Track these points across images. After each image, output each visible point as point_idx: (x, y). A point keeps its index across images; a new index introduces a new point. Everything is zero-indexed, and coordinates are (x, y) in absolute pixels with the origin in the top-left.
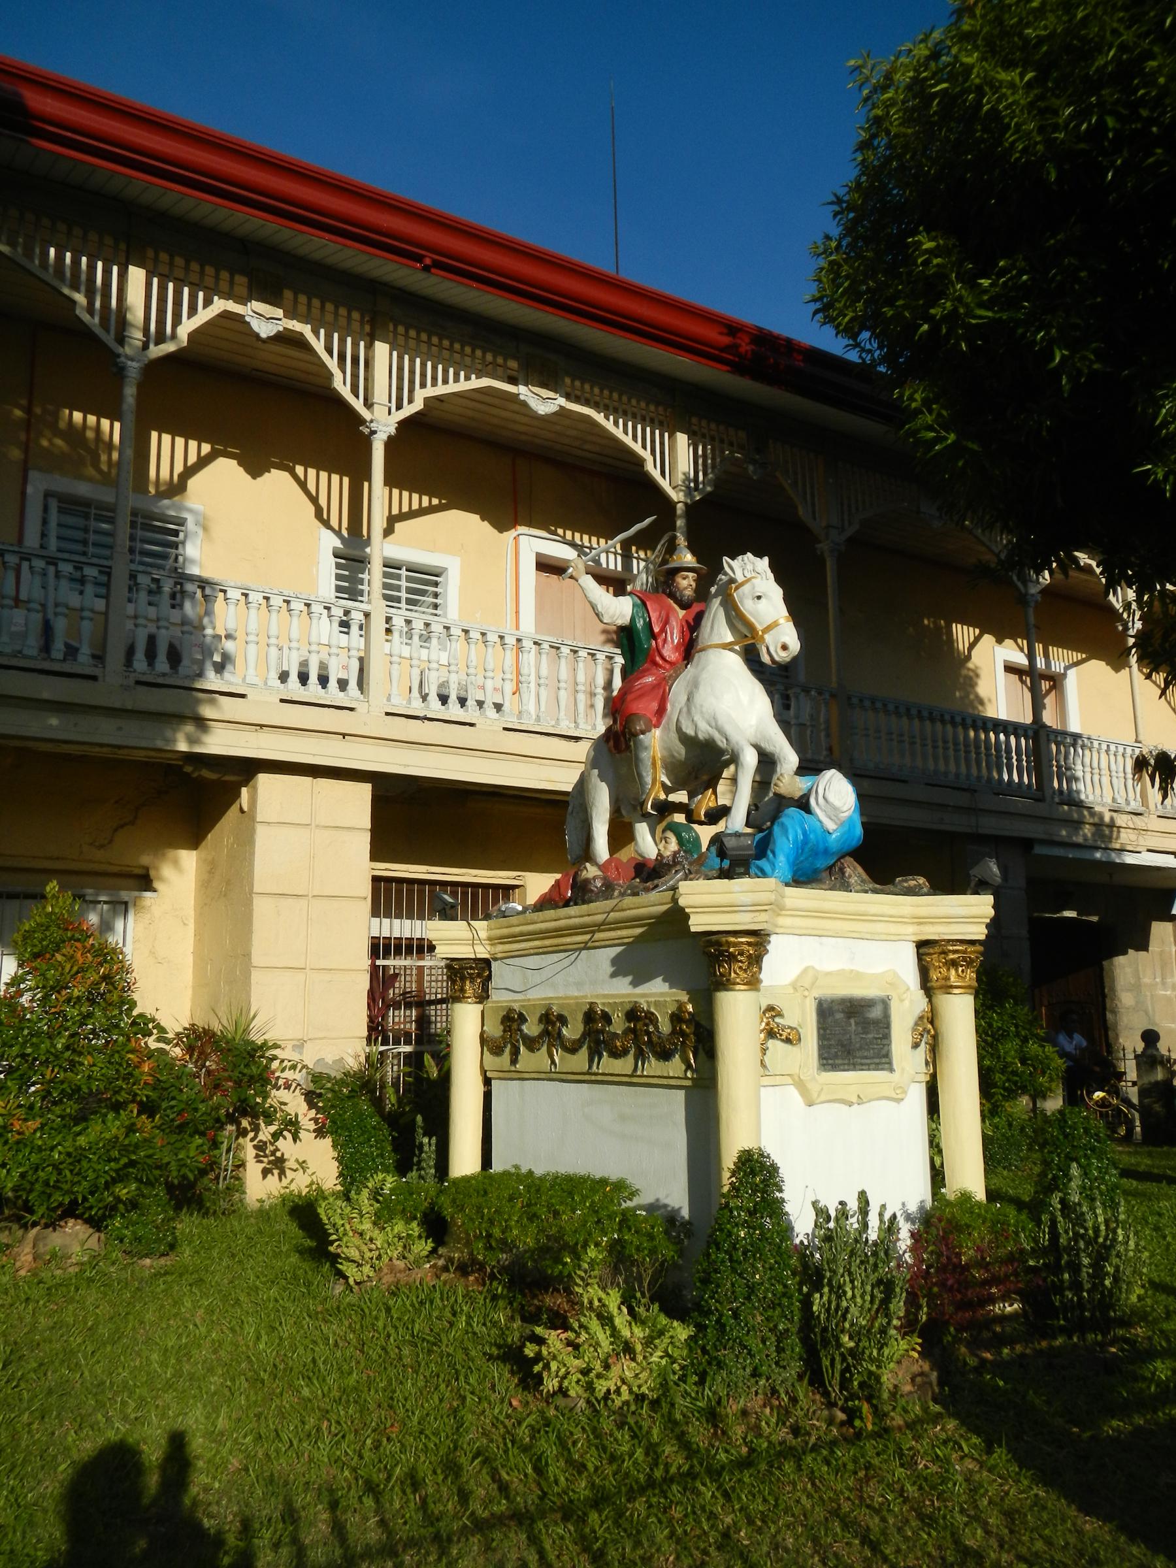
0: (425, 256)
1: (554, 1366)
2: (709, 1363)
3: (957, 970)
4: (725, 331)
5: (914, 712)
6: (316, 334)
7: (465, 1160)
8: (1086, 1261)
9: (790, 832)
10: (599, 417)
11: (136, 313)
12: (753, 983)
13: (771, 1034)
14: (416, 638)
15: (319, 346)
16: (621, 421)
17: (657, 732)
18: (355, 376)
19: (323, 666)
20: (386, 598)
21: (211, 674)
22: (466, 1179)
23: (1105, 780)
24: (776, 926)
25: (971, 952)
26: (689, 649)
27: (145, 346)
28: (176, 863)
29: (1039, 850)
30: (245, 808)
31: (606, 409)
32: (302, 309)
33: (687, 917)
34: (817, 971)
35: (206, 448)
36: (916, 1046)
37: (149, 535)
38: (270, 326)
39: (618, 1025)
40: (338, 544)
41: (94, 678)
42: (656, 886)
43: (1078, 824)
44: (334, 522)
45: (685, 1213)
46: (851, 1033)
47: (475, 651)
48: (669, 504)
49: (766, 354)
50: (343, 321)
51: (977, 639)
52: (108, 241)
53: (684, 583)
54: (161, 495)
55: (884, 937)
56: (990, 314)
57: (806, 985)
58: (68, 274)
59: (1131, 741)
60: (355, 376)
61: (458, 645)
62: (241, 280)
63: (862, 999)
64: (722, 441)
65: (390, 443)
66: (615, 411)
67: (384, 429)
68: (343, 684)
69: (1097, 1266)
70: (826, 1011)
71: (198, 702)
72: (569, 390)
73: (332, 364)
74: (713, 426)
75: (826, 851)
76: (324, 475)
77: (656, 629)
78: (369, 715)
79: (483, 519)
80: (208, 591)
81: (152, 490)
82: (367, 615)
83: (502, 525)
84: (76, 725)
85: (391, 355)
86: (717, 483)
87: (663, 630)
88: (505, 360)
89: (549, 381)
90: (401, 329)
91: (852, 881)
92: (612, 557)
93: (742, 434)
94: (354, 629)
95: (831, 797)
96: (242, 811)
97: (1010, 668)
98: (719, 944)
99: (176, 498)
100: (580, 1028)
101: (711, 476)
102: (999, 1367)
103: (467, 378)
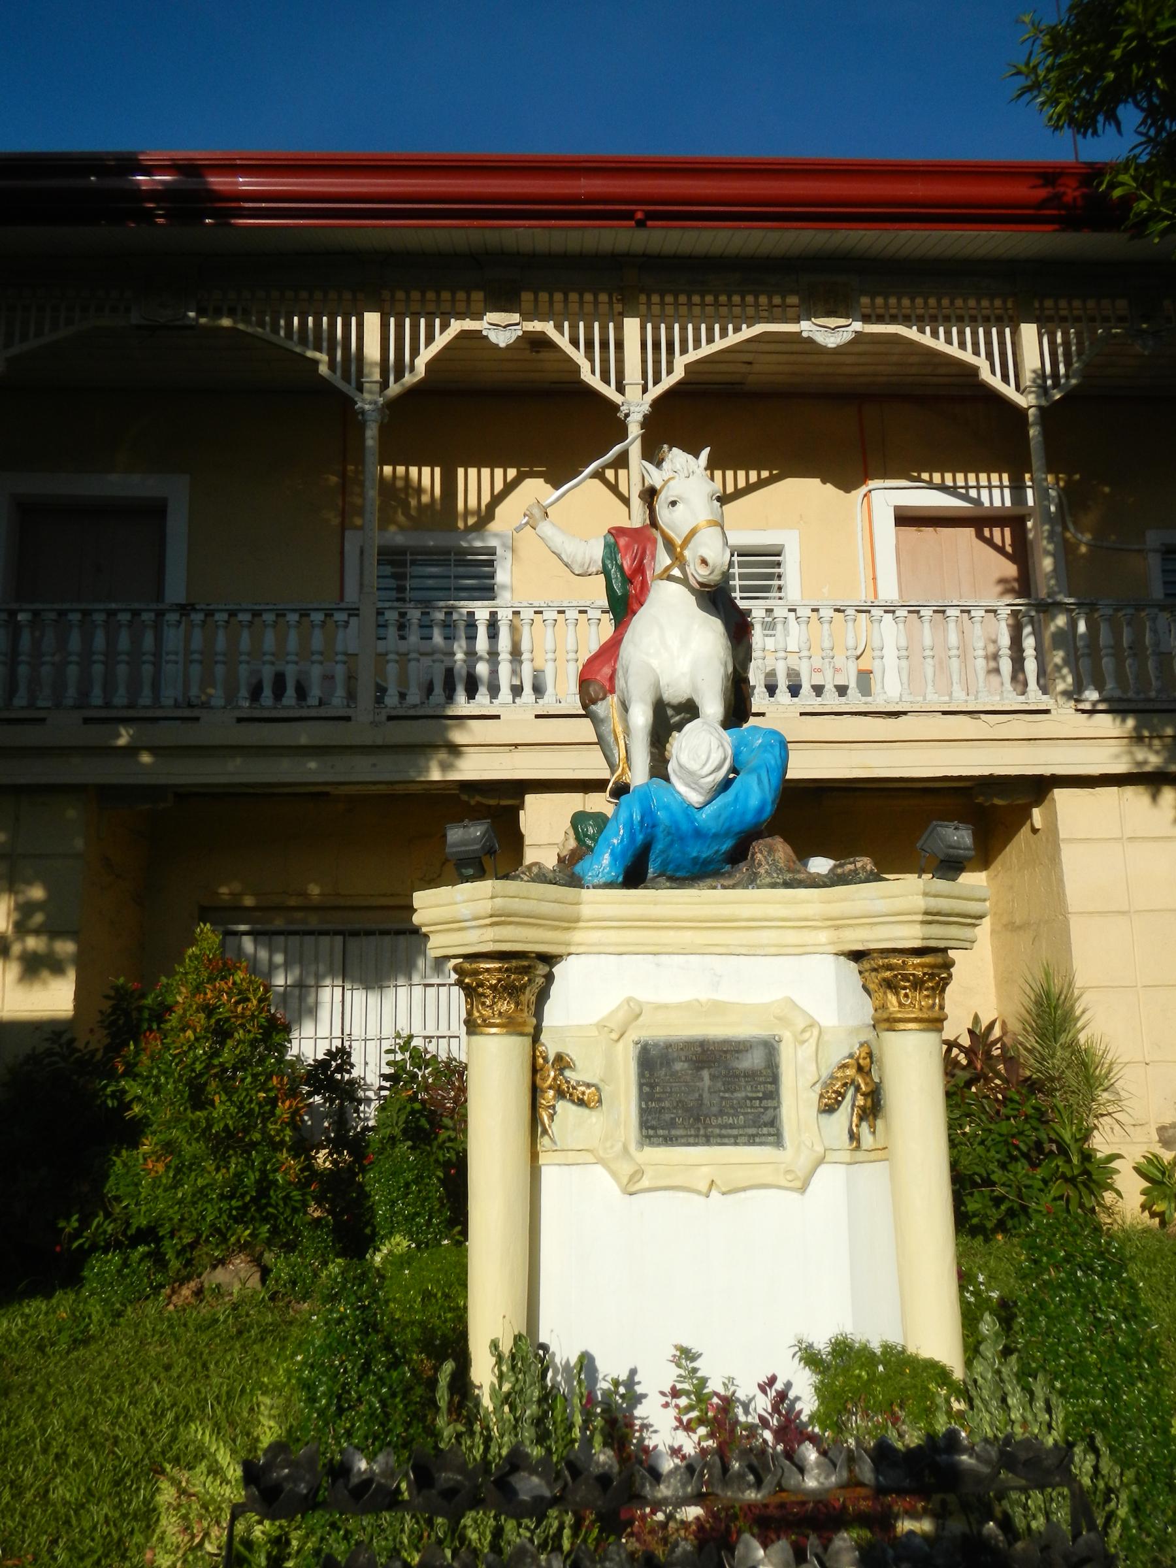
0: (635, 211)
3: (897, 994)
4: (1040, 182)
6: (559, 328)
10: (911, 333)
15: (563, 342)
16: (941, 330)
18: (605, 361)
21: (461, 696)
24: (569, 944)
25: (915, 966)
27: (384, 385)
31: (920, 321)
34: (639, 1003)
35: (512, 473)
36: (829, 1109)
37: (462, 570)
38: (508, 333)
41: (348, 719)
46: (705, 1092)
48: (1019, 413)
50: (589, 308)
52: (347, 295)
54: (469, 530)
55: (773, 950)
57: (612, 1025)
58: (311, 337)
60: (605, 361)
62: (478, 296)
63: (726, 1042)
65: (647, 422)
67: (637, 409)
70: (654, 1063)
71: (446, 728)
72: (868, 311)
73: (579, 356)
75: (698, 834)
79: (824, 482)
81: (461, 525)
83: (847, 486)
84: (333, 767)
85: (643, 329)
86: (1086, 375)
88: (784, 298)
90: (655, 298)
92: (996, 492)
93: (1122, 304)
101: (1076, 365)
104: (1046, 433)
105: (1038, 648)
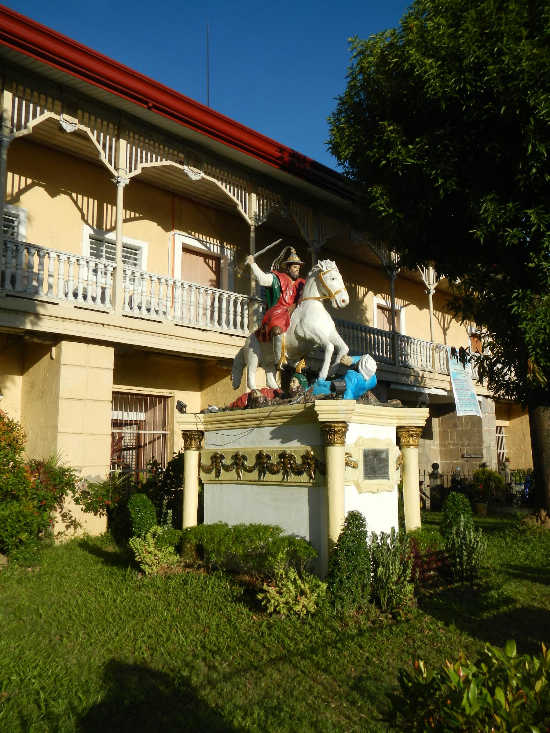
1: (273, 601)
2: (335, 598)
5: (346, 324)
6: (93, 133)
7: (190, 520)
8: (465, 553)
9: (351, 381)
10: (219, 183)
11: (8, 115)
12: (343, 443)
13: (347, 464)
14: (128, 279)
15: (94, 138)
17: (285, 334)
18: (110, 156)
19: (85, 290)
20: (124, 262)
22: (192, 528)
23: (419, 357)
26: (297, 299)
28: (13, 381)
29: (393, 386)
30: (54, 356)
31: (222, 180)
32: (86, 120)
33: (318, 415)
35: (29, 181)
36: (397, 469)
39: (274, 460)
40: (92, 232)
42: (290, 401)
43: (408, 375)
44: (90, 222)
45: (308, 539)
46: (374, 464)
47: (163, 288)
49: (295, 162)
50: (105, 128)
51: (367, 293)
53: (295, 269)
56: (413, 161)
59: (429, 341)
60: (110, 156)
61: (155, 285)
64: (270, 199)
65: (126, 188)
66: (226, 181)
68: (94, 299)
69: (470, 556)
71: (36, 305)
73: (100, 148)
74: (267, 191)
75: (364, 389)
76: (85, 199)
77: (283, 289)
78: (115, 316)
79: (159, 225)
80: (41, 253)
82: (115, 269)
83: (167, 229)
86: (269, 217)
87: (286, 289)
89: (197, 164)
90: (132, 134)
91: (372, 401)
92: (215, 247)
94: (109, 275)
95: (368, 366)
96: (52, 358)
97: (379, 307)
98: (331, 426)
99: (16, 204)
100: (254, 461)
102: (439, 595)
103: (161, 160)
104: (256, 235)
105: (248, 314)
